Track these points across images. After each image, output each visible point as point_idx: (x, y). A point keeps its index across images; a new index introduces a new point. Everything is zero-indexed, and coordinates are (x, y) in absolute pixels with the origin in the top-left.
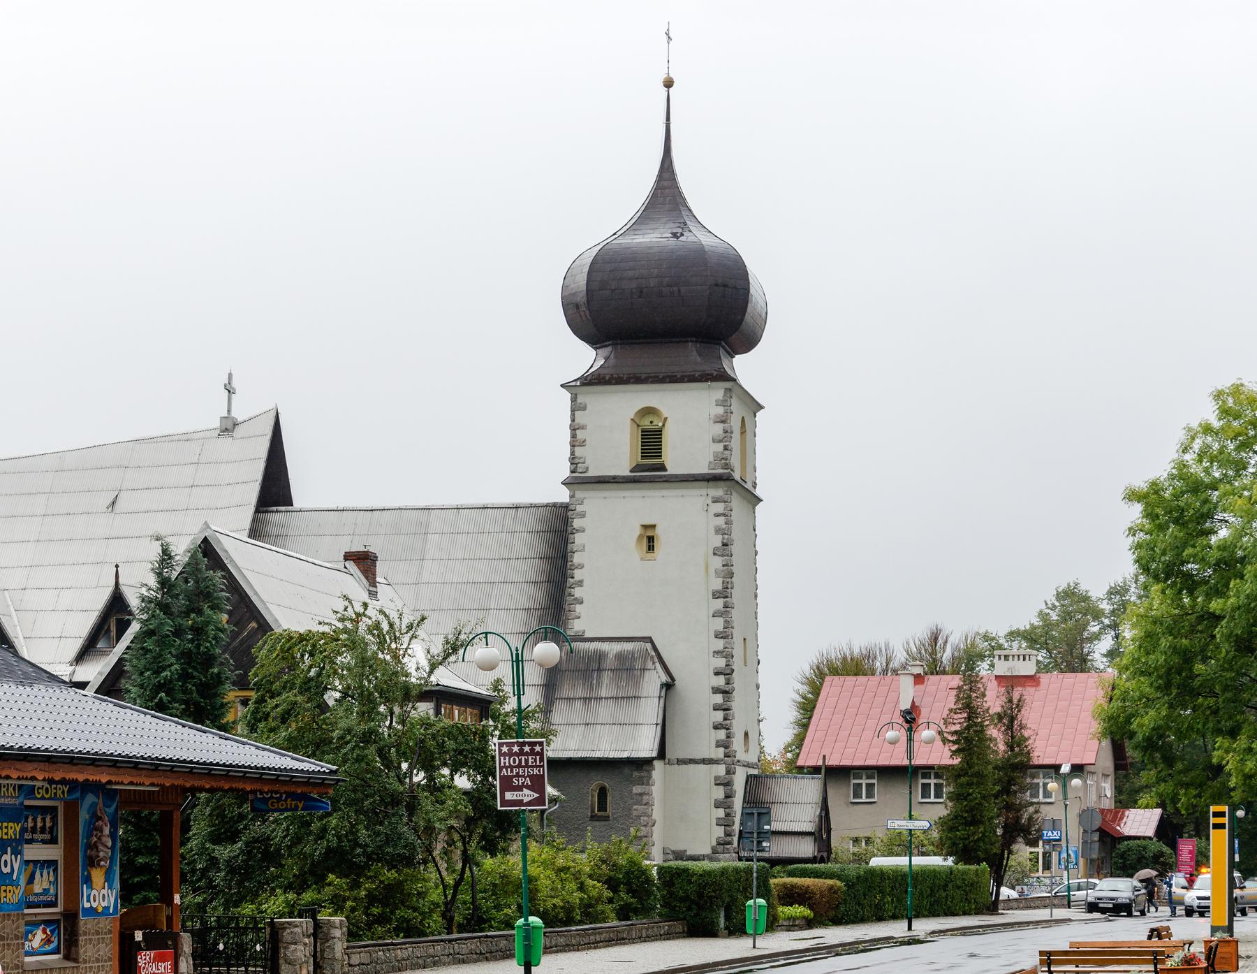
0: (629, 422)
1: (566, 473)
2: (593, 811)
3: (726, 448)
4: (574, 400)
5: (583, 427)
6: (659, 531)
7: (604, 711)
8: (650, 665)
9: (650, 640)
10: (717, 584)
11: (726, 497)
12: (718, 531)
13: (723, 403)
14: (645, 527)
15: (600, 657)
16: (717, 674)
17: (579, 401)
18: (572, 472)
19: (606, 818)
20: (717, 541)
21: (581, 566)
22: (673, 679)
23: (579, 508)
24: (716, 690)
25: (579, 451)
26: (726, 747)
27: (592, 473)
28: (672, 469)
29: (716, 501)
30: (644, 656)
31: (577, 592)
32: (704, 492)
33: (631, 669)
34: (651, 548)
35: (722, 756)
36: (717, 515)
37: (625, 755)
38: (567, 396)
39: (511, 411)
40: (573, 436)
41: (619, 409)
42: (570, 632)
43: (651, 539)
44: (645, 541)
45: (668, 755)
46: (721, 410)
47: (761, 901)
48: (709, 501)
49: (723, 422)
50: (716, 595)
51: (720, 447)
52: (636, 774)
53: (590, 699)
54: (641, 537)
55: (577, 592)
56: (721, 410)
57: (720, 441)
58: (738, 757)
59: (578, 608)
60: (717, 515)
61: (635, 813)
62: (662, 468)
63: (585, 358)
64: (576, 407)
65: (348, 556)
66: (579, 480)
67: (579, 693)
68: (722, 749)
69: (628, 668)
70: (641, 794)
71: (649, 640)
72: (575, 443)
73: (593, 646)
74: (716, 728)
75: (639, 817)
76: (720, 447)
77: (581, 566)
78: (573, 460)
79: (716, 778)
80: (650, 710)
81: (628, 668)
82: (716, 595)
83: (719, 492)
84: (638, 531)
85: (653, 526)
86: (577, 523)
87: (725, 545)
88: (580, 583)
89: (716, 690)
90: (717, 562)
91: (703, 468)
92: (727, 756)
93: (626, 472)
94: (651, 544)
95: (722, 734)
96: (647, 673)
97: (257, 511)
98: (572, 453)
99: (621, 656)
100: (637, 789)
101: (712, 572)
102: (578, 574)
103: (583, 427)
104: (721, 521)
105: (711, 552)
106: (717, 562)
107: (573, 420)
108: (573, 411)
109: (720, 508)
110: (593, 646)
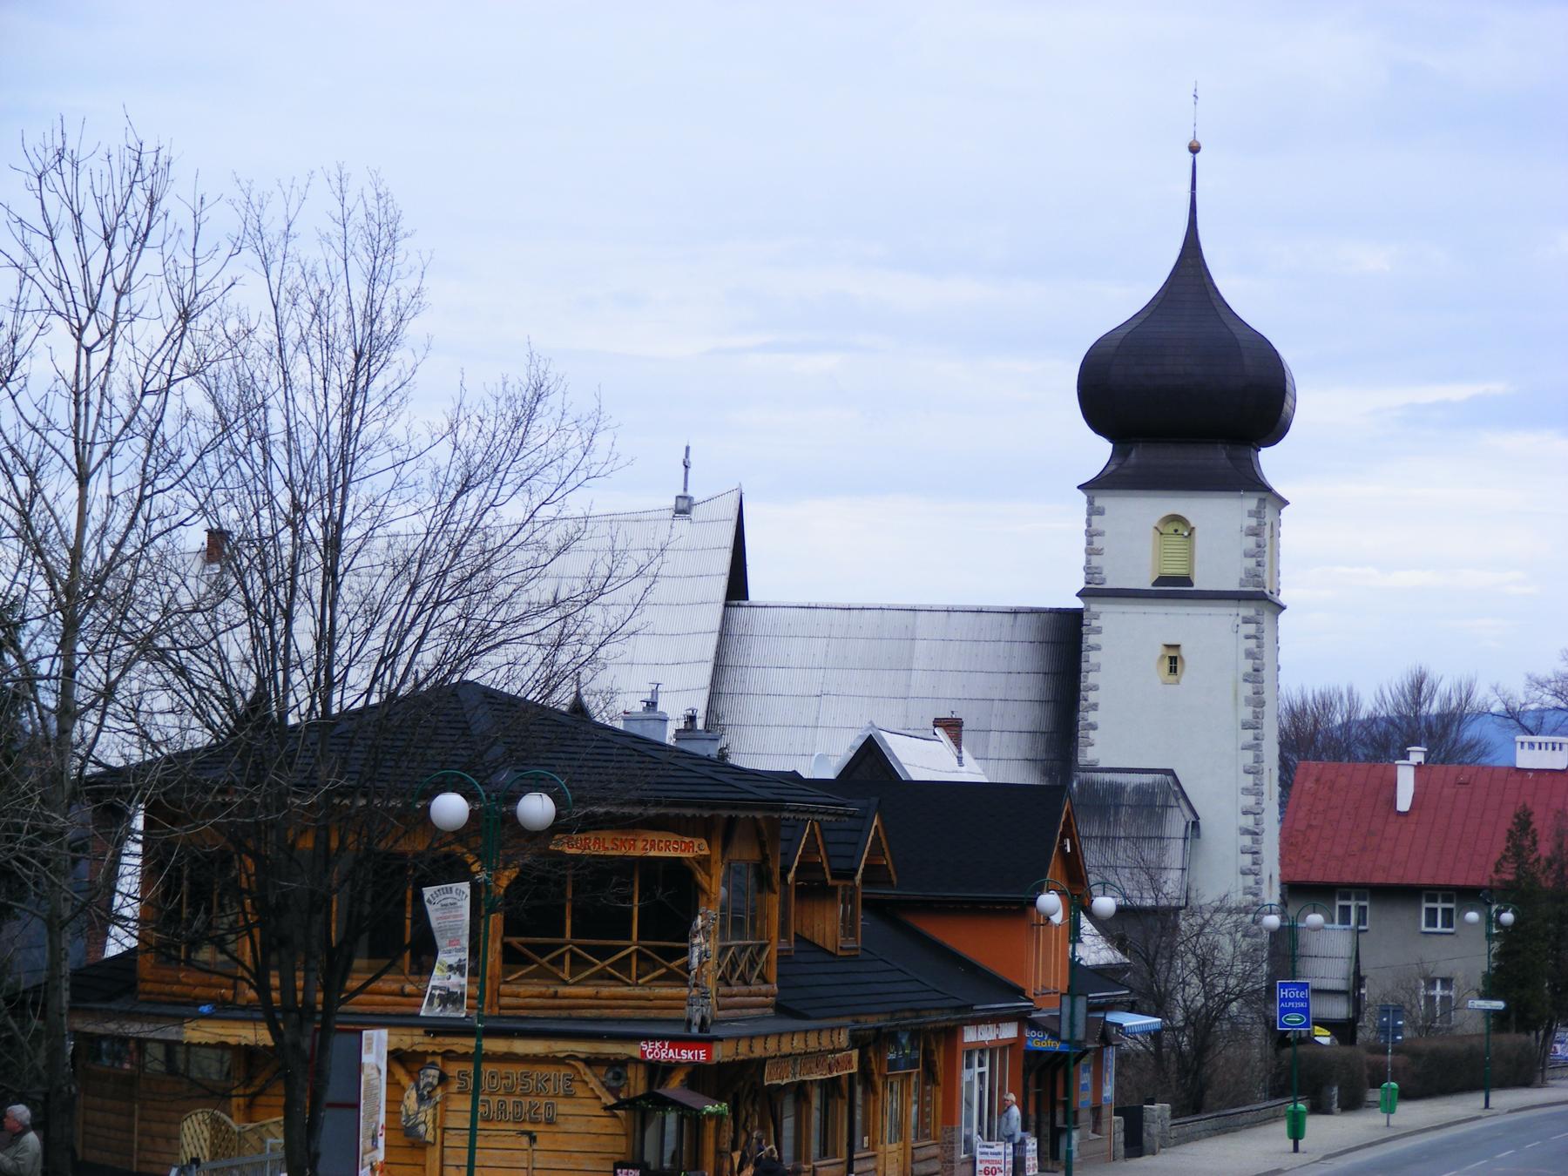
0: (1152, 530)
1: (1081, 585)
3: (1259, 564)
4: (1090, 502)
5: (1100, 534)
6: (1184, 652)
8: (1172, 801)
10: (1247, 713)
12: (1250, 654)
13: (1257, 513)
14: (1168, 646)
15: (1117, 789)
16: (1245, 813)
20: (1247, 666)
21: (1095, 688)
23: (1095, 623)
24: (1245, 832)
25: (1096, 560)
26: (1256, 895)
27: (1110, 584)
28: (1199, 584)
29: (1246, 621)
31: (1092, 717)
32: (1234, 611)
33: (1152, 806)
34: (1173, 670)
36: (1247, 637)
38: (1082, 497)
39: (1027, 517)
40: (1090, 543)
41: (1141, 512)
42: (1082, 760)
44: (1167, 662)
46: (1253, 522)
47: (1394, 1085)
48: (1239, 621)
50: (1246, 726)
51: (1251, 563)
54: (1163, 657)
55: (1092, 717)
56: (1253, 522)
59: (1092, 734)
60: (1247, 637)
62: (1187, 581)
63: (1097, 452)
64: (1093, 511)
65: (938, 723)
68: (1250, 897)
71: (1170, 772)
72: (1091, 551)
73: (1108, 777)
74: (1244, 873)
76: (1251, 563)
77: (1095, 688)
78: (1090, 570)
82: (1246, 726)
83: (1248, 610)
84: (1159, 651)
85: (1177, 647)
86: (1090, 639)
87: (1256, 670)
88: (1095, 707)
89: (1245, 832)
90: (1247, 689)
91: (1233, 585)
93: (1148, 586)
94: (1174, 664)
95: (1250, 880)
96: (1170, 811)
97: (726, 606)
98: (1088, 562)
99: (1139, 790)
101: (1242, 700)
102: (1092, 697)
103: (1100, 534)
104: (1252, 643)
105: (1241, 677)
106: (1247, 689)
107: (1089, 525)
108: (1090, 514)
110: (1108, 777)
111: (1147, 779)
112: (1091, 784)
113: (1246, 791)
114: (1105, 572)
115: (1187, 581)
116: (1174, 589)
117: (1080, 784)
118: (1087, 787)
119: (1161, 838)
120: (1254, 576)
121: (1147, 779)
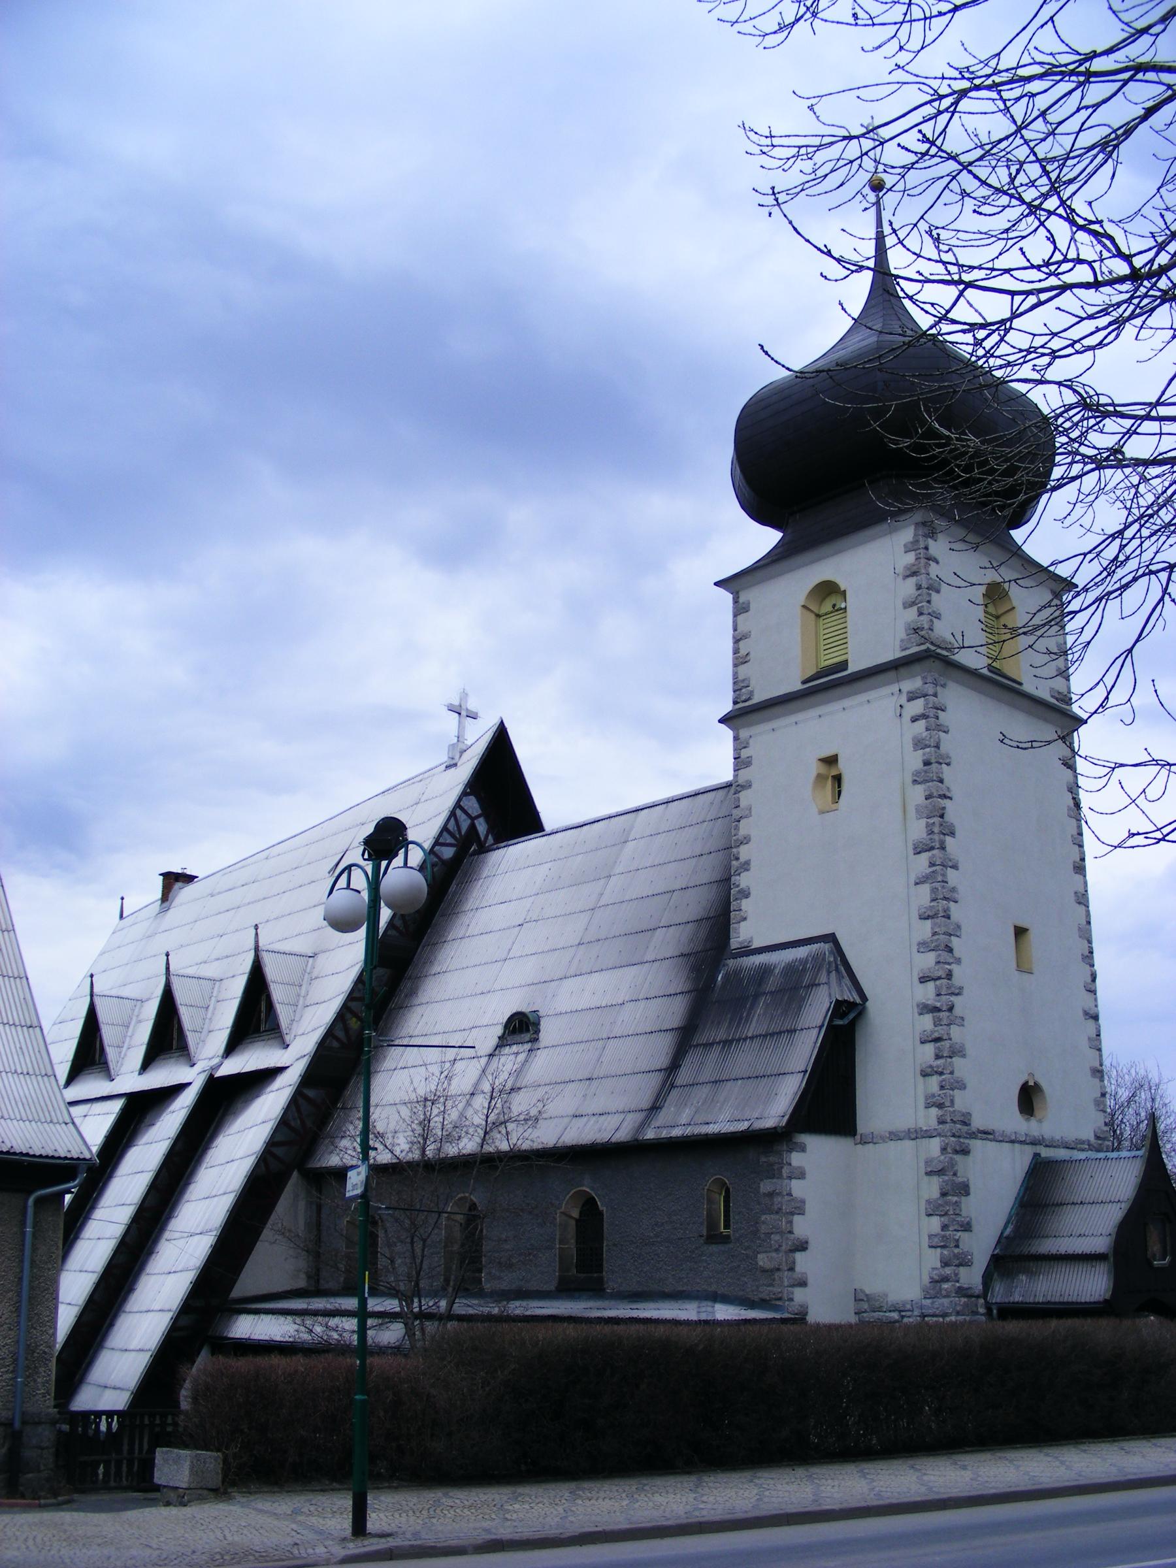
0: (799, 610)
1: (727, 707)
2: (712, 1224)
4: (736, 601)
6: (843, 766)
7: (745, 1059)
8: (823, 978)
9: (831, 938)
11: (930, 689)
12: (919, 744)
15: (765, 971)
16: (923, 980)
17: (741, 600)
18: (735, 703)
19: (725, 1239)
20: (915, 760)
22: (864, 998)
24: (925, 1009)
26: (940, 1106)
27: (756, 699)
29: (912, 698)
30: (817, 961)
32: (895, 688)
35: (933, 1123)
37: (743, 1126)
38: (726, 597)
40: (736, 651)
42: (734, 943)
43: (838, 779)
45: (862, 1127)
48: (903, 699)
49: (914, 574)
52: (763, 1159)
53: (731, 1042)
54: (820, 778)
56: (911, 558)
57: (913, 604)
58: (978, 1123)
59: (745, 904)
61: (763, 1229)
63: (770, 537)
64: (740, 609)
66: (742, 715)
67: (721, 1035)
68: (934, 1111)
69: (794, 986)
70: (771, 1195)
72: (740, 660)
74: (925, 1074)
75: (769, 1235)
76: (912, 613)
78: (740, 686)
79: (928, 1162)
80: (803, 1050)
81: (794, 986)
84: (815, 768)
87: (927, 763)
89: (925, 1009)
90: (917, 794)
92: (941, 1122)
93: (799, 686)
100: (766, 1186)
105: (909, 779)
107: (735, 630)
108: (735, 616)
109: (918, 706)
111: (801, 952)
112: (737, 972)
113: (924, 947)
114: (753, 683)
115: (843, 665)
116: (830, 682)
117: (727, 977)
118: (735, 977)
119: (792, 1031)
121: (801, 952)
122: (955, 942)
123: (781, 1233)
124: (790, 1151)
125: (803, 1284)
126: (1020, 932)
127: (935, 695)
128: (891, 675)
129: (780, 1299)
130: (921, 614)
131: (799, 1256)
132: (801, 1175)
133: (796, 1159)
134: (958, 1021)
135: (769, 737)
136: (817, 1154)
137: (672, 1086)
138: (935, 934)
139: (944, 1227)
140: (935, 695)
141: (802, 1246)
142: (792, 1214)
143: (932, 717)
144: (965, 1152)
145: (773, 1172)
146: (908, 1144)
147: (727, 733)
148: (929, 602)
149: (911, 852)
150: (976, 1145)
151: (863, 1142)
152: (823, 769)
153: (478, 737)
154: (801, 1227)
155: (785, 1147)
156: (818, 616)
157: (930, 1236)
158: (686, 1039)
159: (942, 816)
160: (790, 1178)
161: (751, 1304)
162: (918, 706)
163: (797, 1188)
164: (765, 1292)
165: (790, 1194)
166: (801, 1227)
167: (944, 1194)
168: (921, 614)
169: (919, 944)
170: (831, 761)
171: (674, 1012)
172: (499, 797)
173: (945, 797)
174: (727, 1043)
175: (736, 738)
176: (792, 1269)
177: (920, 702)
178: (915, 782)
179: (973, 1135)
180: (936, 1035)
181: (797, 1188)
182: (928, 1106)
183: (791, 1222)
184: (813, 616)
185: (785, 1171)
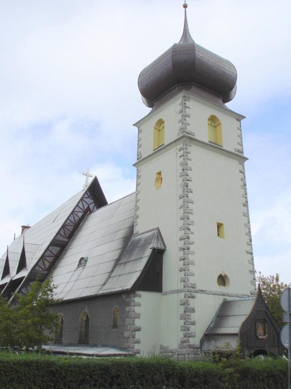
0: (153, 129)
1: (135, 161)
6: (163, 175)
9: (158, 230)
15: (140, 240)
16: (181, 239)
17: (140, 129)
26: (184, 281)
38: (136, 129)
45: (164, 290)
48: (177, 151)
58: (198, 287)
60: (180, 157)
61: (126, 323)
70: (128, 312)
72: (139, 146)
75: (127, 325)
78: (139, 154)
83: (180, 146)
87: (183, 170)
91: (176, 138)
100: (127, 309)
109: (181, 153)
115: (163, 145)
116: (160, 149)
119: (141, 258)
120: (182, 130)
122: (191, 227)
123: (130, 325)
124: (135, 297)
125: (138, 342)
126: (219, 226)
127: (186, 149)
128: (174, 144)
129: (129, 348)
130: (183, 124)
131: (137, 333)
132: (139, 305)
133: (137, 300)
134: (192, 253)
135: (144, 168)
136: (145, 298)
137: (110, 277)
138: (184, 224)
139: (185, 323)
140: (186, 149)
141: (139, 329)
142: (135, 318)
143: (185, 156)
144: (193, 297)
145: (128, 304)
146: (176, 295)
147: (135, 169)
148: (185, 120)
149: (178, 198)
150: (197, 295)
151: (164, 295)
152: (158, 176)
153: (91, 180)
154: (138, 323)
155: (132, 296)
156: (159, 130)
157: (181, 327)
158: (118, 262)
159: (187, 186)
160: (134, 306)
161: (122, 349)
162: (181, 153)
163: (137, 310)
164: (126, 345)
165: (134, 312)
166: (138, 323)
167: (185, 312)
168: (183, 124)
169: (180, 228)
170: (159, 173)
171: (115, 255)
172: (95, 195)
173: (189, 180)
174: (126, 263)
175: (137, 170)
176: (134, 337)
177: (182, 151)
178: (180, 176)
179: (197, 292)
180: (184, 257)
181: (137, 310)
182: (181, 282)
183: (134, 321)
184: (158, 131)
185: (133, 303)
